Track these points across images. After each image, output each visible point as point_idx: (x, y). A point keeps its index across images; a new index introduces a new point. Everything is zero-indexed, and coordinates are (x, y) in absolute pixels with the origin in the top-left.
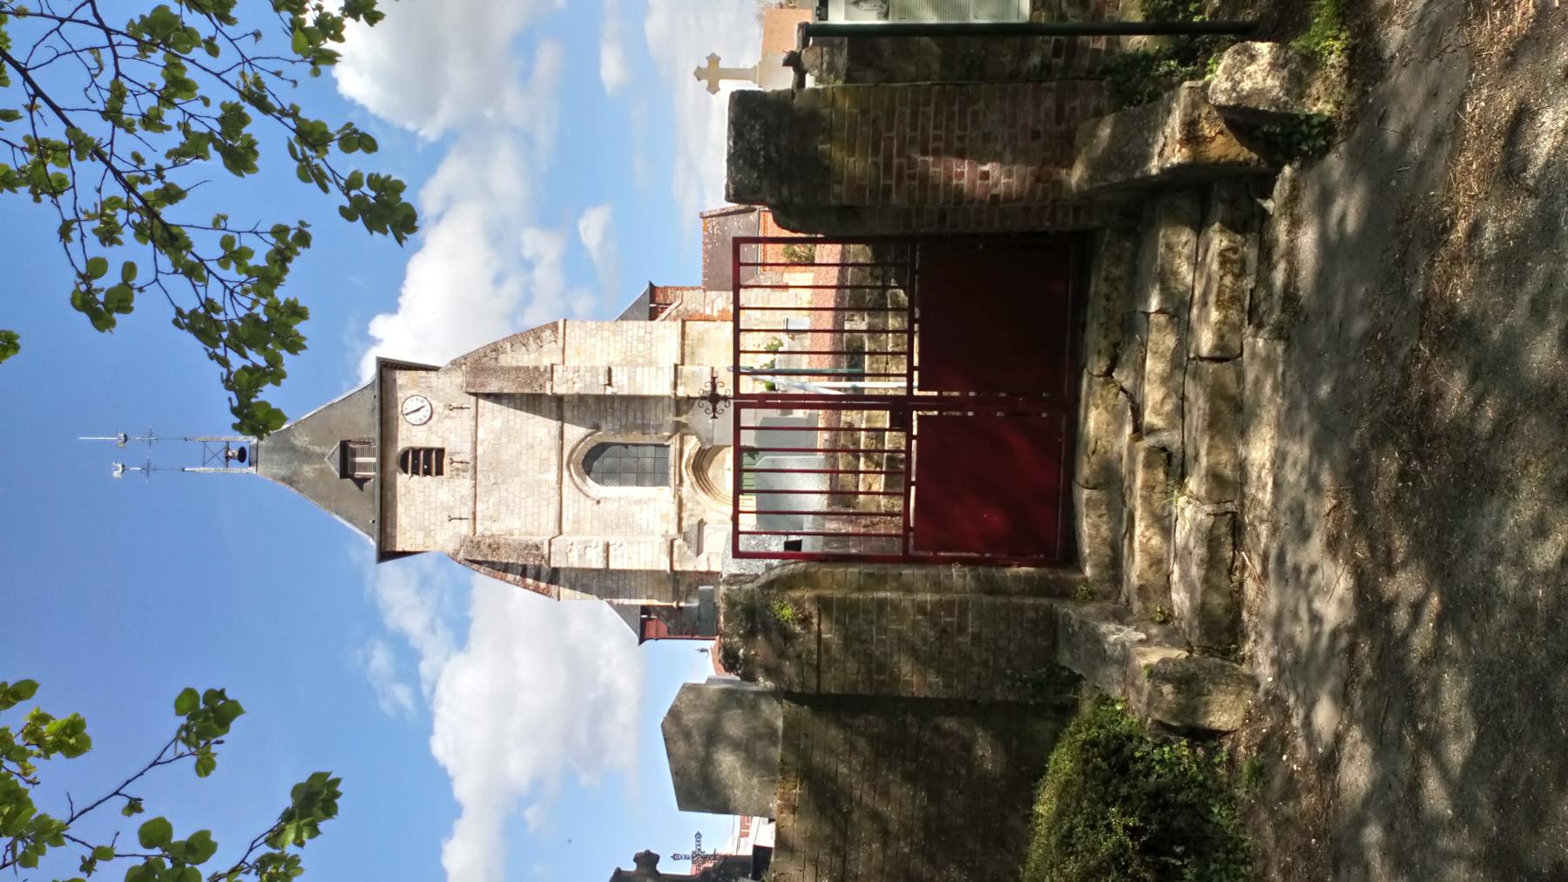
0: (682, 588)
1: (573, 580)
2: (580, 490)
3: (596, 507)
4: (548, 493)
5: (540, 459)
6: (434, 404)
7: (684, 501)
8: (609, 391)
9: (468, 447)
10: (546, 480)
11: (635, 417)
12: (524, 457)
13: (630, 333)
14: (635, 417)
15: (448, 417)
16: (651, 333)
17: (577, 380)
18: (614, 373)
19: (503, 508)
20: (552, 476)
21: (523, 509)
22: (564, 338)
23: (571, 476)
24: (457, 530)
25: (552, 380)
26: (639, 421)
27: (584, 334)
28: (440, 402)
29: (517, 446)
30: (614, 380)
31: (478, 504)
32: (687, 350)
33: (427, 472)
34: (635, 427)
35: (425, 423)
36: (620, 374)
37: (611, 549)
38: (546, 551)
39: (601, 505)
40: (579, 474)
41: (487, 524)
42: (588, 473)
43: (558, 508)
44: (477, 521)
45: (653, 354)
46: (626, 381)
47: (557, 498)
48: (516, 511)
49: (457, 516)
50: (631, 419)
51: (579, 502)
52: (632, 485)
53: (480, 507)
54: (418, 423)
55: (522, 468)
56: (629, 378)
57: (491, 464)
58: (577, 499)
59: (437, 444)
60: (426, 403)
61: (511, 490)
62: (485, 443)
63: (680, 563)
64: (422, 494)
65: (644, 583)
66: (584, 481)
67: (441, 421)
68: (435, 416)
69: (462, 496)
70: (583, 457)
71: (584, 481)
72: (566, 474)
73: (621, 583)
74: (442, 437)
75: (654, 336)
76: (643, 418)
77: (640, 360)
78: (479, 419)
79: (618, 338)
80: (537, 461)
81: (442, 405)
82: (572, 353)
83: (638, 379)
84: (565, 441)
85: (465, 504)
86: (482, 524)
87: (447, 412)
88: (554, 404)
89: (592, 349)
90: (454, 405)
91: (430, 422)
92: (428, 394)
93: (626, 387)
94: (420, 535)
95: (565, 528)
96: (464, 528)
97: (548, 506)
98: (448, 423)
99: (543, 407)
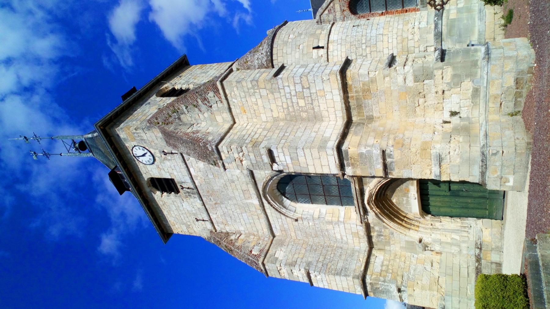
7: (372, 225)
10: (252, 204)
13: (287, 90)
15: (165, 159)
16: (309, 88)
20: (256, 202)
22: (227, 99)
23: (269, 203)
24: (204, 226)
25: (221, 159)
27: (243, 94)
32: (352, 103)
36: (281, 155)
37: (311, 275)
39: (299, 222)
40: (276, 199)
41: (222, 226)
42: (284, 194)
43: (266, 221)
44: (214, 224)
45: (316, 109)
46: (289, 161)
47: (263, 216)
48: (238, 221)
51: (281, 218)
52: (322, 204)
54: (148, 163)
55: (231, 195)
56: (291, 158)
57: (208, 192)
58: (280, 217)
60: (146, 151)
61: (229, 208)
66: (281, 203)
70: (276, 185)
71: (281, 203)
75: (313, 91)
77: (304, 115)
78: (187, 162)
79: (277, 95)
82: (238, 111)
83: (302, 159)
84: (256, 179)
89: (255, 107)
93: (290, 166)
95: (277, 233)
97: (259, 219)
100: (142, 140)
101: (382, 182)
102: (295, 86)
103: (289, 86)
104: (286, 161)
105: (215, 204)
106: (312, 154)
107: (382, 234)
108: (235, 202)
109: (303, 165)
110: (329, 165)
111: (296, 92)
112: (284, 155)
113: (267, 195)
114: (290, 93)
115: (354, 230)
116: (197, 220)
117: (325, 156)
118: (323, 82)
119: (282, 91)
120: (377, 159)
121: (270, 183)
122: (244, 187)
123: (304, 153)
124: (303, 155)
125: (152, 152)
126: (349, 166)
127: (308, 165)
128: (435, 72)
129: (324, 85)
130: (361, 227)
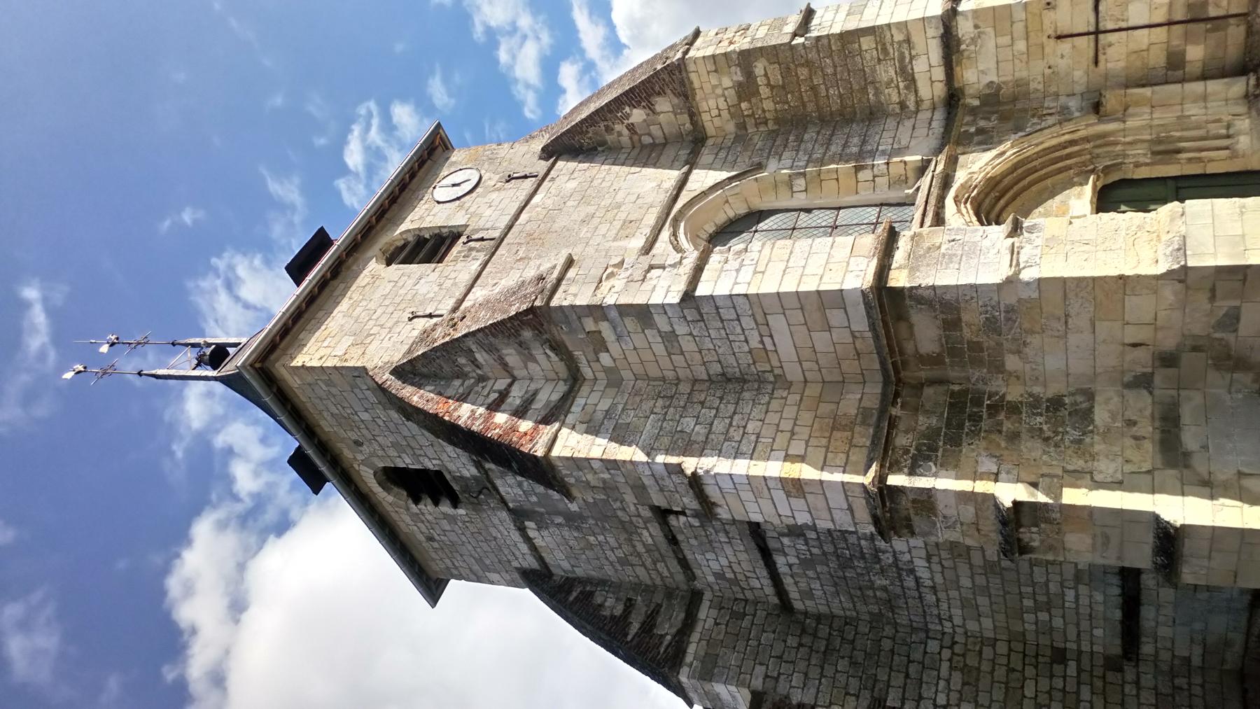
0: (902, 440)
1: (599, 415)
12: (596, 221)
23: (675, 234)
26: (855, 150)
29: (591, 209)
31: (473, 290)
34: (842, 158)
35: (458, 198)
62: (539, 209)
63: (913, 270)
65: (786, 425)
68: (479, 190)
73: (719, 426)
76: (864, 142)
78: (546, 183)
80: (617, 224)
91: (467, 198)
98: (494, 195)
101: (1008, 154)
113: (682, 225)
121: (710, 198)
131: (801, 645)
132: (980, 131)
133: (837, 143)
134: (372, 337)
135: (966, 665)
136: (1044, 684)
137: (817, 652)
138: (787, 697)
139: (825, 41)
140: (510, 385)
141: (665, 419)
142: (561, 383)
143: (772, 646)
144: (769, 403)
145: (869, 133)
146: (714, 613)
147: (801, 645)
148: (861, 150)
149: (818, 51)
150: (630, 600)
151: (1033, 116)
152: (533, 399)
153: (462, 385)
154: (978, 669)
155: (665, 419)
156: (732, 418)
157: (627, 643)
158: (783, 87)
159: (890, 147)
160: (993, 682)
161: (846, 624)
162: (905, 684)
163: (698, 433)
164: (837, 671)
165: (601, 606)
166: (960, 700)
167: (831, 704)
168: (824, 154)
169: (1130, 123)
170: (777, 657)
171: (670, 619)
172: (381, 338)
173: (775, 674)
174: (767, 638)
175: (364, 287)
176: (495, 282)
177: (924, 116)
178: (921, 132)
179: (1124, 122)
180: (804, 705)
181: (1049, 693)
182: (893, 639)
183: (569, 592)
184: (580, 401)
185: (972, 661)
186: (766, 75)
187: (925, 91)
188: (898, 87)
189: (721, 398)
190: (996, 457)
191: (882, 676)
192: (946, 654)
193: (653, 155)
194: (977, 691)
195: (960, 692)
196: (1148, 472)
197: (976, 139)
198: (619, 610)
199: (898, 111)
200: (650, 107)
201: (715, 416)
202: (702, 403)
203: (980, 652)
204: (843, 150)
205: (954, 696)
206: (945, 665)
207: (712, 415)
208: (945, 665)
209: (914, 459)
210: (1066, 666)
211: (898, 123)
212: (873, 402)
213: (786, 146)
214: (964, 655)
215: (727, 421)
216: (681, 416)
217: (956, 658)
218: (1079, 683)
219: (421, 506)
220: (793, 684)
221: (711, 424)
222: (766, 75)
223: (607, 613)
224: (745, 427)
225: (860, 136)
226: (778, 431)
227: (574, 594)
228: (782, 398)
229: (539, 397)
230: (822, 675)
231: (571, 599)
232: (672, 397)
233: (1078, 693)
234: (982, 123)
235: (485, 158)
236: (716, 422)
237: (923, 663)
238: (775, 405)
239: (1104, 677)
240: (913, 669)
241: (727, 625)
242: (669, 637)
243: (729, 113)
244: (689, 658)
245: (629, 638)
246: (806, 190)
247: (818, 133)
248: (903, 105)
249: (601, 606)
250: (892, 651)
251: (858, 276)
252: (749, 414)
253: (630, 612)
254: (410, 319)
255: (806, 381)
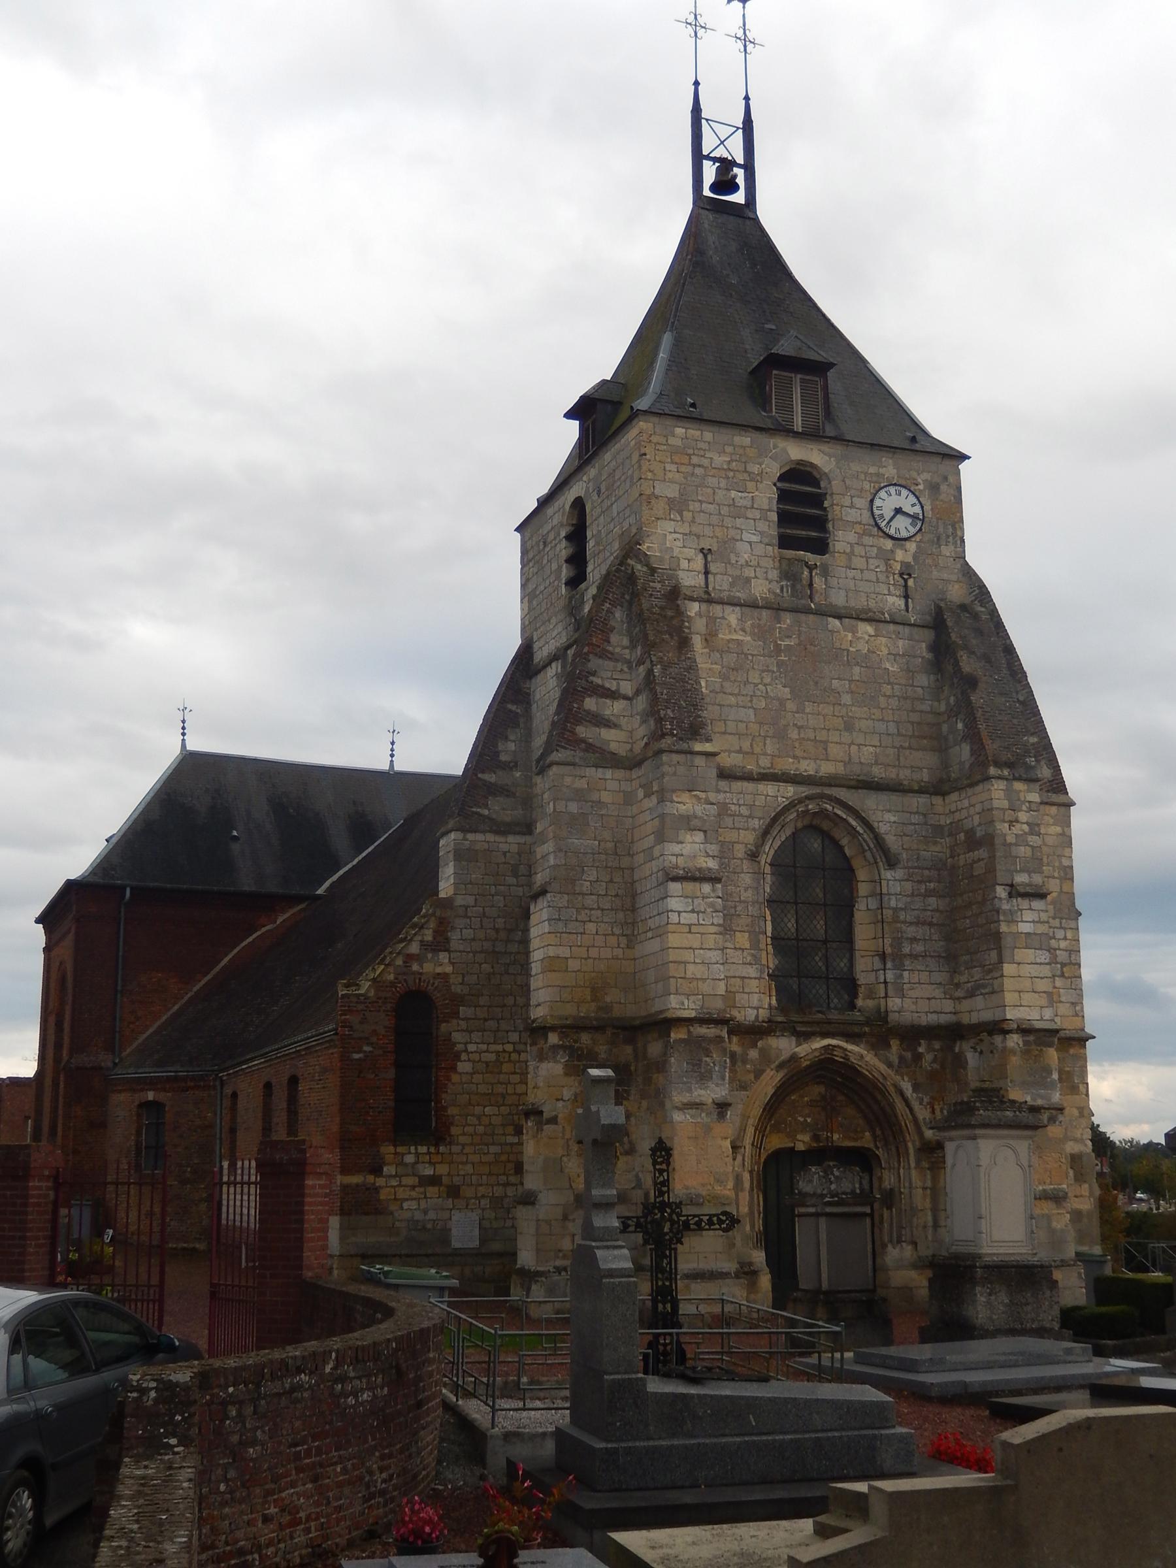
0: (585, 1038)
1: (595, 796)
2: (774, 820)
3: (740, 851)
4: (765, 754)
5: (825, 742)
6: (912, 546)
8: (1001, 892)
9: (838, 599)
11: (914, 940)
13: (1060, 934)
14: (914, 940)
15: (889, 570)
17: (1017, 829)
18: (1037, 904)
19: (730, 659)
21: (733, 700)
24: (684, 564)
28: (915, 557)
30: (1024, 903)
33: (784, 518)
37: (706, 888)
38: (698, 747)
46: (1025, 928)
49: (713, 568)
50: (911, 931)
51: (750, 816)
53: (732, 616)
54: (877, 512)
59: (842, 540)
64: (749, 504)
65: (594, 953)
67: (886, 558)
68: (889, 544)
69: (748, 580)
72: (804, 791)
73: (590, 901)
74: (852, 552)
76: (914, 957)
80: (822, 736)
81: (910, 559)
83: (1029, 954)
85: (732, 584)
86: (699, 614)
87: (897, 567)
88: (925, 776)
90: (911, 582)
92: (927, 537)
94: (672, 491)
96: (690, 579)
97: (740, 751)
99: (919, 754)
100: (939, 539)
102: (1066, 951)
103: (1065, 938)
104: (1022, 921)
105: (777, 646)
106: (1042, 978)
107: (739, 1064)
108: (790, 706)
109: (1020, 954)
110: (1021, 1006)
111: (1055, 949)
112: (1033, 922)
114: (1054, 938)
115: (741, 999)
116: (705, 553)
117: (1038, 1003)
118: (1073, 1003)
119: (1056, 923)
120: (1042, 1097)
122: (834, 750)
123: (1041, 964)
124: (1038, 961)
125: (908, 544)
126: (1026, 1043)
127: (1019, 964)
128: (1086, 1186)
129: (1068, 1005)
130: (753, 1018)
131: (497, 931)
132: (918, 1057)
133: (917, 932)
134: (679, 519)
135: (502, 1063)
136: (496, 1120)
137: (494, 946)
138: (453, 928)
139: (995, 918)
140: (626, 698)
141: (593, 854)
142: (628, 747)
143: (493, 906)
144: (613, 934)
145: (929, 959)
146: (514, 849)
147: (497, 931)
148: (905, 956)
149: (990, 911)
150: (516, 765)
151: (932, 1098)
152: (610, 727)
153: (625, 648)
154: (500, 1073)
155: (593, 854)
156: (599, 908)
157: (476, 775)
158: (972, 876)
159: (906, 981)
160: (492, 1084)
161: (522, 966)
162: (480, 1019)
163: (582, 885)
164: (480, 964)
165: (506, 739)
166: (474, 1062)
167: (453, 964)
168: (904, 922)
169: (914, 1173)
170: (484, 913)
171: (503, 809)
172: (677, 530)
173: (470, 914)
174: (499, 901)
175: (745, 471)
176: (748, 630)
177: (948, 1005)
178: (923, 1006)
179: (915, 1168)
180: (448, 942)
181: (490, 1124)
182: (515, 1005)
183: (514, 702)
184: (609, 774)
185: (506, 1067)
186: (979, 860)
187: (966, 1005)
188: (968, 982)
189: (617, 895)
190: (576, 1097)
191: (483, 1001)
192: (509, 1047)
193: (925, 741)
194: (483, 1073)
195: (480, 1061)
196: (571, 1186)
197: (908, 1055)
198: (504, 758)
199: (956, 981)
200: (965, 738)
201: (599, 895)
202: (611, 881)
203: (515, 1073)
204: (907, 938)
205: (476, 1057)
206: (499, 1048)
207: (600, 892)
208: (499, 1048)
209: (571, 1047)
210: (514, 1135)
211: (940, 984)
212: (617, 1012)
213: (920, 882)
214: (510, 1061)
215: (595, 906)
216: (597, 867)
217: (507, 1055)
218: (501, 1144)
219: (564, 543)
220: (464, 931)
221: (591, 894)
222: (979, 860)
223: (501, 747)
224: (590, 921)
225: (925, 951)
226: (588, 947)
227: (514, 708)
228: (619, 944)
229: (613, 731)
230: (475, 953)
231: (509, 706)
232: (616, 854)
233: (493, 1144)
234: (929, 1057)
235: (941, 530)
236: (593, 897)
237: (498, 1031)
238: (613, 940)
239: (509, 1161)
240: (492, 1024)
241: (505, 863)
242: (486, 812)
243: (959, 821)
244: (470, 836)
245: (479, 775)
246: (868, 909)
247: (937, 910)
248: (957, 985)
249: (506, 739)
250: (505, 1006)
251: (683, 1004)
252: (602, 922)
253: (504, 769)
254: (702, 550)
255: (635, 959)
